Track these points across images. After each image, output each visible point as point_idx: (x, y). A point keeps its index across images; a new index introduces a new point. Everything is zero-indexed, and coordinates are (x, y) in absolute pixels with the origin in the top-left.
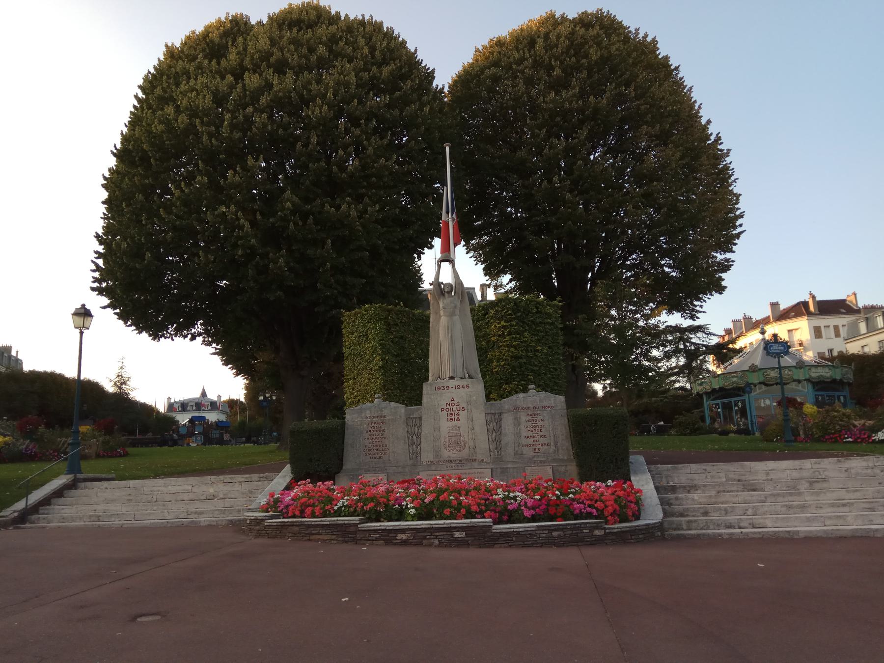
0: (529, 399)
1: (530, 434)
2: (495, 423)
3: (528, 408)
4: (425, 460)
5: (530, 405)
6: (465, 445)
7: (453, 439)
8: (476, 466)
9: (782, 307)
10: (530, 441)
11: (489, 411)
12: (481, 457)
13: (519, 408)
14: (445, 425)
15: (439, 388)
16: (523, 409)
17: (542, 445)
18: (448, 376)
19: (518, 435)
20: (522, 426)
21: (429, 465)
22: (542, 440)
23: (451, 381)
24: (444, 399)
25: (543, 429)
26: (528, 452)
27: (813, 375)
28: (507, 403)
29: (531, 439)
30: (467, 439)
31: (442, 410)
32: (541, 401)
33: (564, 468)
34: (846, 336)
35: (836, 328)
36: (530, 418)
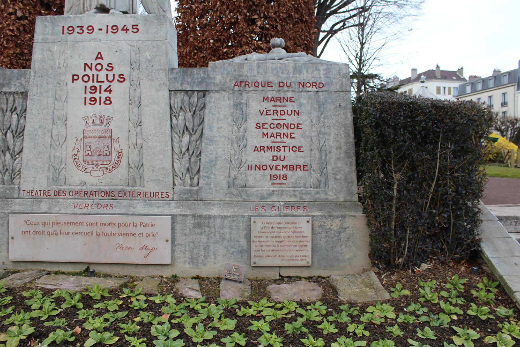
0: (270, 64)
1: (267, 142)
2: (189, 116)
3: (268, 84)
4: (29, 188)
5: (271, 78)
6: (119, 158)
7: (95, 145)
8: (139, 207)
9: (419, 73)
10: (266, 158)
12: (151, 187)
13: (247, 84)
14: (79, 112)
15: (71, 30)
16: (256, 84)
17: (292, 168)
18: (94, 4)
19: (240, 142)
20: (251, 125)
21: (35, 197)
22: (292, 158)
24: (80, 53)
25: (297, 133)
26: (260, 183)
28: (219, 71)
29: (269, 154)
31: (75, 78)
32: (297, 70)
33: (337, 221)
34: (456, 94)
35: (449, 89)
36: (269, 105)
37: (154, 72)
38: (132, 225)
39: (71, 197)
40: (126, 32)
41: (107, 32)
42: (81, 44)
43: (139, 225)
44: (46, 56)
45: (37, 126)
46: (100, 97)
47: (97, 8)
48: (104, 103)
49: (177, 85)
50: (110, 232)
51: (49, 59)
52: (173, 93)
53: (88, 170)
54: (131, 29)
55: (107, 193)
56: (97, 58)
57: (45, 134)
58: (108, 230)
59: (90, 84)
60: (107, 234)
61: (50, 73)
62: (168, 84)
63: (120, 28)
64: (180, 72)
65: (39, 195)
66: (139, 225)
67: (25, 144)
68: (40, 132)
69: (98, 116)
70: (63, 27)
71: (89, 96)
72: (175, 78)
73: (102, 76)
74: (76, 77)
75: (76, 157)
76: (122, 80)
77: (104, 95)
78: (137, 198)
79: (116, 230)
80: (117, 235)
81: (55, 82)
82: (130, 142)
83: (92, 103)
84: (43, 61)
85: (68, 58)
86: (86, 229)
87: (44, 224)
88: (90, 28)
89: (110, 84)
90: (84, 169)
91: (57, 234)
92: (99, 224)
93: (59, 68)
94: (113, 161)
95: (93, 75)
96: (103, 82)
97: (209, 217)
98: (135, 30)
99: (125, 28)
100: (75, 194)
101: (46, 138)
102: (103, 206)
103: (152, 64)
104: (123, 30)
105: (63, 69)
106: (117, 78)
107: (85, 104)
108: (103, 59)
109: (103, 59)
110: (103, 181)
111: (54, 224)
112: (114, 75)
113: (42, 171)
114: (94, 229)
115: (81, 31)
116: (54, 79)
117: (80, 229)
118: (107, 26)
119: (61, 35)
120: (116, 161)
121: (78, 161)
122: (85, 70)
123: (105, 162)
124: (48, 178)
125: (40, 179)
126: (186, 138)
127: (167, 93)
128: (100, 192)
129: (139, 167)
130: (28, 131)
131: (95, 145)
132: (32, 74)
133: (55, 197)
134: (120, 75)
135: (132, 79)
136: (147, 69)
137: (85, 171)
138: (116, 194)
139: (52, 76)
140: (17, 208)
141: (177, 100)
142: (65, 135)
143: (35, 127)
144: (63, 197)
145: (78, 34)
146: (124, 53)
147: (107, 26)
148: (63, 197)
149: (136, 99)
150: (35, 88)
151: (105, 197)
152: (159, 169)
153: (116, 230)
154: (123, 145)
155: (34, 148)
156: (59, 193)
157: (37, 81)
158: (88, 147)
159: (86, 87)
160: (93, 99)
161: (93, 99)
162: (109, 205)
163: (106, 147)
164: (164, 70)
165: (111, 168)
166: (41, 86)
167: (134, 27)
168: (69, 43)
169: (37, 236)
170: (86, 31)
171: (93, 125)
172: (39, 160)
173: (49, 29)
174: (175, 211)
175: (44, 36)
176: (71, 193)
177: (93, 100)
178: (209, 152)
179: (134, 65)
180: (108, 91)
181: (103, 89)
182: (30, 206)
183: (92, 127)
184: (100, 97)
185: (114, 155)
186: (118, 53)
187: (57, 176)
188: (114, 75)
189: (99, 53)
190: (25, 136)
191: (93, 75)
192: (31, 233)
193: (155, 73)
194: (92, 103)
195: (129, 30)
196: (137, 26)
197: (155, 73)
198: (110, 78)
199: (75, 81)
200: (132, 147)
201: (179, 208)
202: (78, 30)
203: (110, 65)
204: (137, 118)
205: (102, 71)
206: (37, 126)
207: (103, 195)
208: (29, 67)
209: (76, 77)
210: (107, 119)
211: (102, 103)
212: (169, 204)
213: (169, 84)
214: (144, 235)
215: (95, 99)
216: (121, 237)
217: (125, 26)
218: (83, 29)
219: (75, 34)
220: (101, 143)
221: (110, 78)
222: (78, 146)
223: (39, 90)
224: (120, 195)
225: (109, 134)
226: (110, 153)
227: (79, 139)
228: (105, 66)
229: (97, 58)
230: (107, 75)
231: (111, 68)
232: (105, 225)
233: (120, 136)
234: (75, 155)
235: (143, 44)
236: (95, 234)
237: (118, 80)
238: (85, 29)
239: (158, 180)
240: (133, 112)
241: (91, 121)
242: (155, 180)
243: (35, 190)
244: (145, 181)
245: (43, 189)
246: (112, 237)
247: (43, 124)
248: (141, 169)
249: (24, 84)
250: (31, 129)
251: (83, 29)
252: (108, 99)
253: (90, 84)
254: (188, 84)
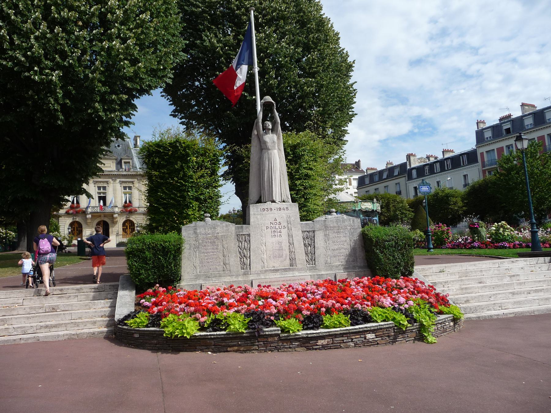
1: (336, 247)
15: (264, 210)
27: (363, 207)
31: (267, 228)
68: (256, 249)
71: (273, 234)
73: (277, 227)
84: (254, 222)
97: (322, 274)
126: (309, 248)
128: (281, 269)
140: (253, 278)
173: (255, 210)
174: (310, 274)
178: (317, 252)
185: (284, 256)
253: (273, 230)
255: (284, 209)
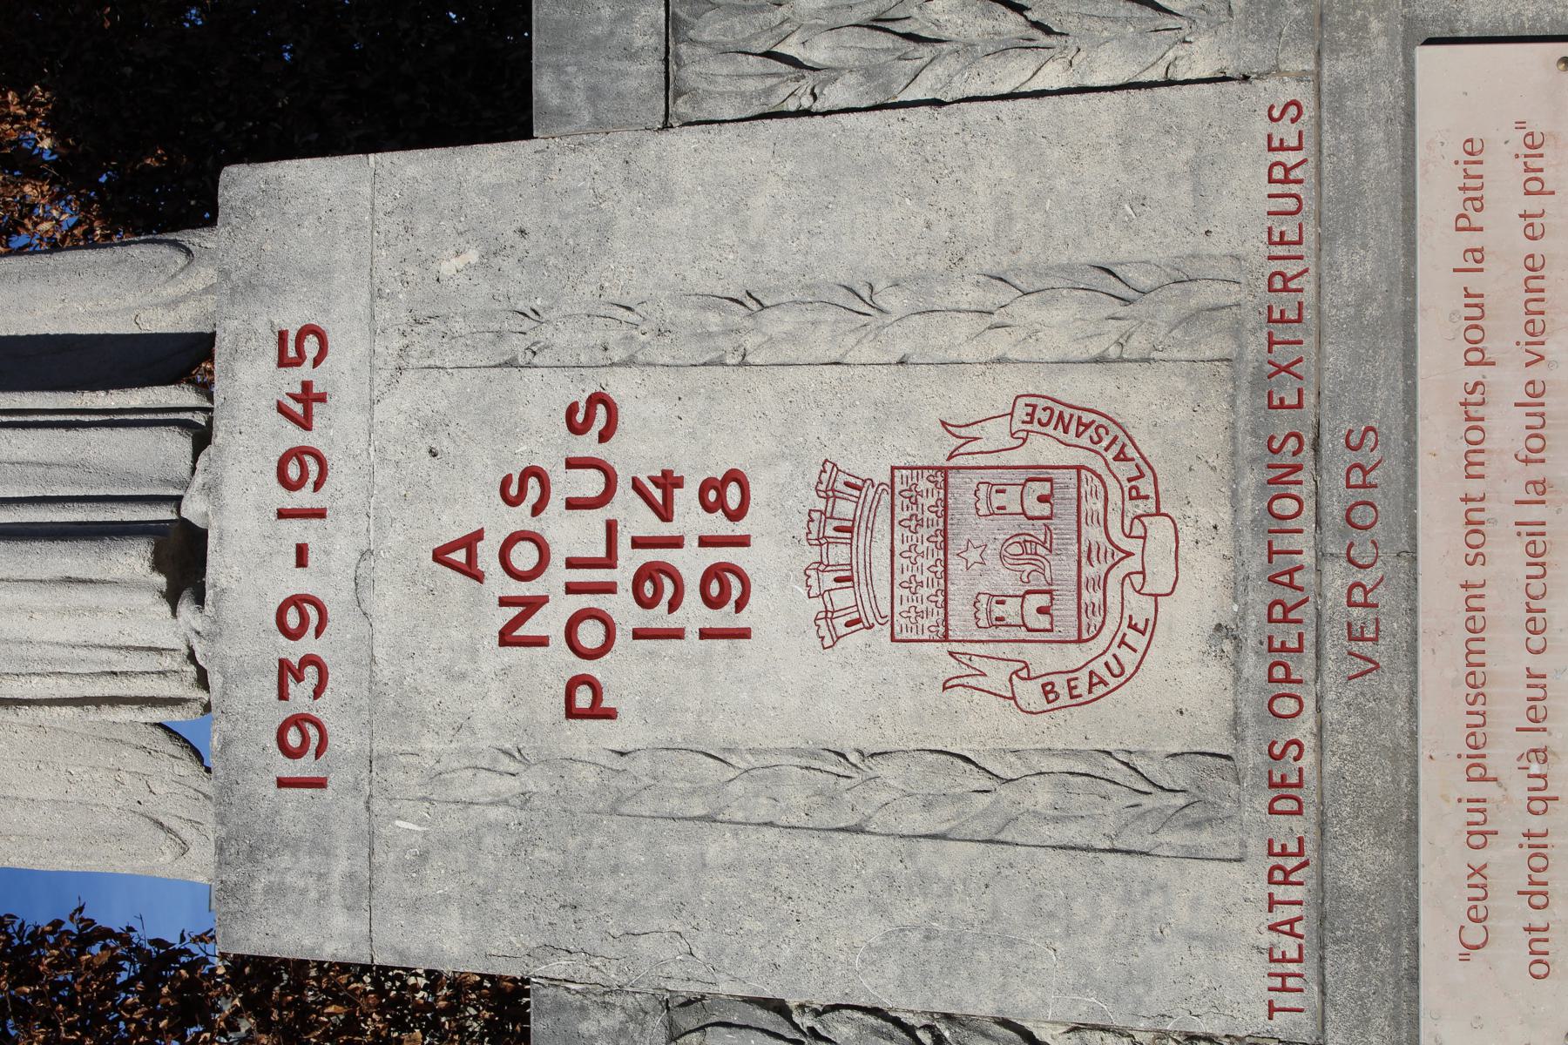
4: (1254, 979)
7: (983, 571)
11: (643, 75)
14: (792, 674)
15: (300, 735)
23: (219, 567)
30: (1003, 389)
31: (586, 704)
37: (555, 221)
38: (1474, 282)
39: (1310, 704)
40: (322, 398)
41: (320, 514)
42: (385, 672)
43: (1474, 240)
44: (450, 887)
45: (875, 930)
46: (705, 542)
47: (172, 597)
48: (735, 516)
49: (632, 83)
50: (1519, 418)
51: (473, 865)
52: (682, 107)
53: (1140, 608)
54: (305, 372)
55: (1282, 477)
56: (471, 571)
57: (923, 880)
58: (1506, 427)
59: (622, 607)
60: (1534, 433)
61: (556, 858)
62: (628, 136)
63: (294, 436)
64: (559, 69)
65: (1295, 911)
66: (1474, 240)
67: (982, 1005)
68: (914, 910)
69: (813, 554)
70: (282, 783)
71: (693, 613)
72: (594, 93)
73: (575, 534)
74: (583, 698)
75: (1060, 683)
76: (601, 410)
77: (690, 518)
78: (1308, 297)
79: (1508, 380)
80: (1536, 372)
81: (612, 824)
82: (968, 353)
83: (736, 592)
84: (479, 903)
85: (467, 752)
86: (1507, 559)
87: (1480, 834)
88: (293, 619)
89: (624, 488)
90: (1132, 637)
91: (1542, 754)
92: (1475, 487)
93: (526, 798)
94: (1080, 457)
95: (571, 589)
96: (611, 527)
98: (311, 346)
99: (298, 408)
100: (1287, 679)
101: (944, 871)
102: (1362, 494)
103: (510, 236)
104: (305, 423)
105: (536, 782)
106: (587, 445)
107: (744, 634)
108: (478, 535)
109: (478, 535)
110: (1208, 519)
111: (1477, 767)
112: (571, 464)
113: (1146, 893)
114: (1502, 513)
115: (311, 672)
116: (592, 826)
117: (1505, 605)
118: (283, 514)
119: (328, 793)
120: (1084, 441)
121: (1084, 676)
122: (542, 642)
123: (1093, 505)
124: (1193, 855)
125: (1196, 904)
127: (684, 141)
129: (1121, 290)
130: (902, 983)
131: (983, 571)
132: (558, 967)
133: (1310, 811)
134: (576, 429)
135: (599, 356)
136: (541, 262)
137: (1146, 629)
138: (1283, 424)
139: (572, 844)
141: (722, 81)
142: (930, 757)
143: (876, 940)
144: (1308, 760)
145: (327, 692)
146: (442, 405)
147: (283, 514)
148: (1308, 760)
149: (713, 320)
150: (644, 945)
151: (1305, 491)
152: (1129, 168)
153: (1508, 380)
154: (985, 398)
155: (1011, 944)
156: (1283, 784)
157: (607, 936)
158: (998, 611)
159: (638, 634)
160: (715, 588)
161: (715, 588)
162: (1351, 457)
163: (998, 500)
164: (546, 167)
165: (1125, 470)
166: (631, 906)
167: (292, 353)
168: (380, 746)
169: (1557, 879)
170: (308, 644)
171: (870, 582)
172: (1080, 910)
173: (292, 869)
175: (335, 897)
176: (1278, 706)
177: (722, 585)
179: (517, 345)
180: (668, 498)
181: (651, 525)
182: (1372, 952)
183: (883, 592)
184: (705, 542)
185: (1045, 449)
186: (444, 444)
187: (1180, 800)
188: (571, 464)
189: (440, 556)
190: (940, 1007)
191: (571, 589)
192: (1538, 919)
193: (564, 216)
194: (736, 592)
195: (306, 386)
196: (282, 336)
197: (564, 216)
198: (591, 483)
199: (604, 704)
200: (1000, 344)
201: (1363, 26)
202: (301, 694)
203: (513, 490)
204: (830, 315)
205: (548, 537)
206: (875, 930)
207: (1292, 506)
208: (520, 987)
209: (583, 698)
210: (830, 494)
211: (739, 529)
212: (1341, 91)
213: (626, 125)
214: (1533, 204)
215: (715, 572)
216: (1550, 349)
217: (282, 409)
218: (295, 661)
219: (323, 708)
220: (978, 532)
221: (591, 483)
222: (997, 677)
223: (658, 922)
224: (1291, 400)
225: (923, 485)
226: (1038, 473)
227: (952, 668)
228: (519, 518)
229: (471, 571)
230: (572, 504)
231: (533, 482)
232: (1475, 447)
233: (935, 417)
234: (1048, 691)
235: (393, 295)
236: (1534, 513)
237: (604, 437)
238: (294, 651)
239: (1195, 169)
240: (792, 338)
241: (843, 597)
242: (1198, 191)
243: (1268, 938)
244: (1206, 246)
245: (1261, 889)
246: (1551, 403)
247: (860, 891)
248: (1132, 274)
249: (619, 1016)
250: (892, 969)
251: (295, 661)
252: (713, 494)
253: (622, 607)
254: (625, 17)
255: (304, 405)
